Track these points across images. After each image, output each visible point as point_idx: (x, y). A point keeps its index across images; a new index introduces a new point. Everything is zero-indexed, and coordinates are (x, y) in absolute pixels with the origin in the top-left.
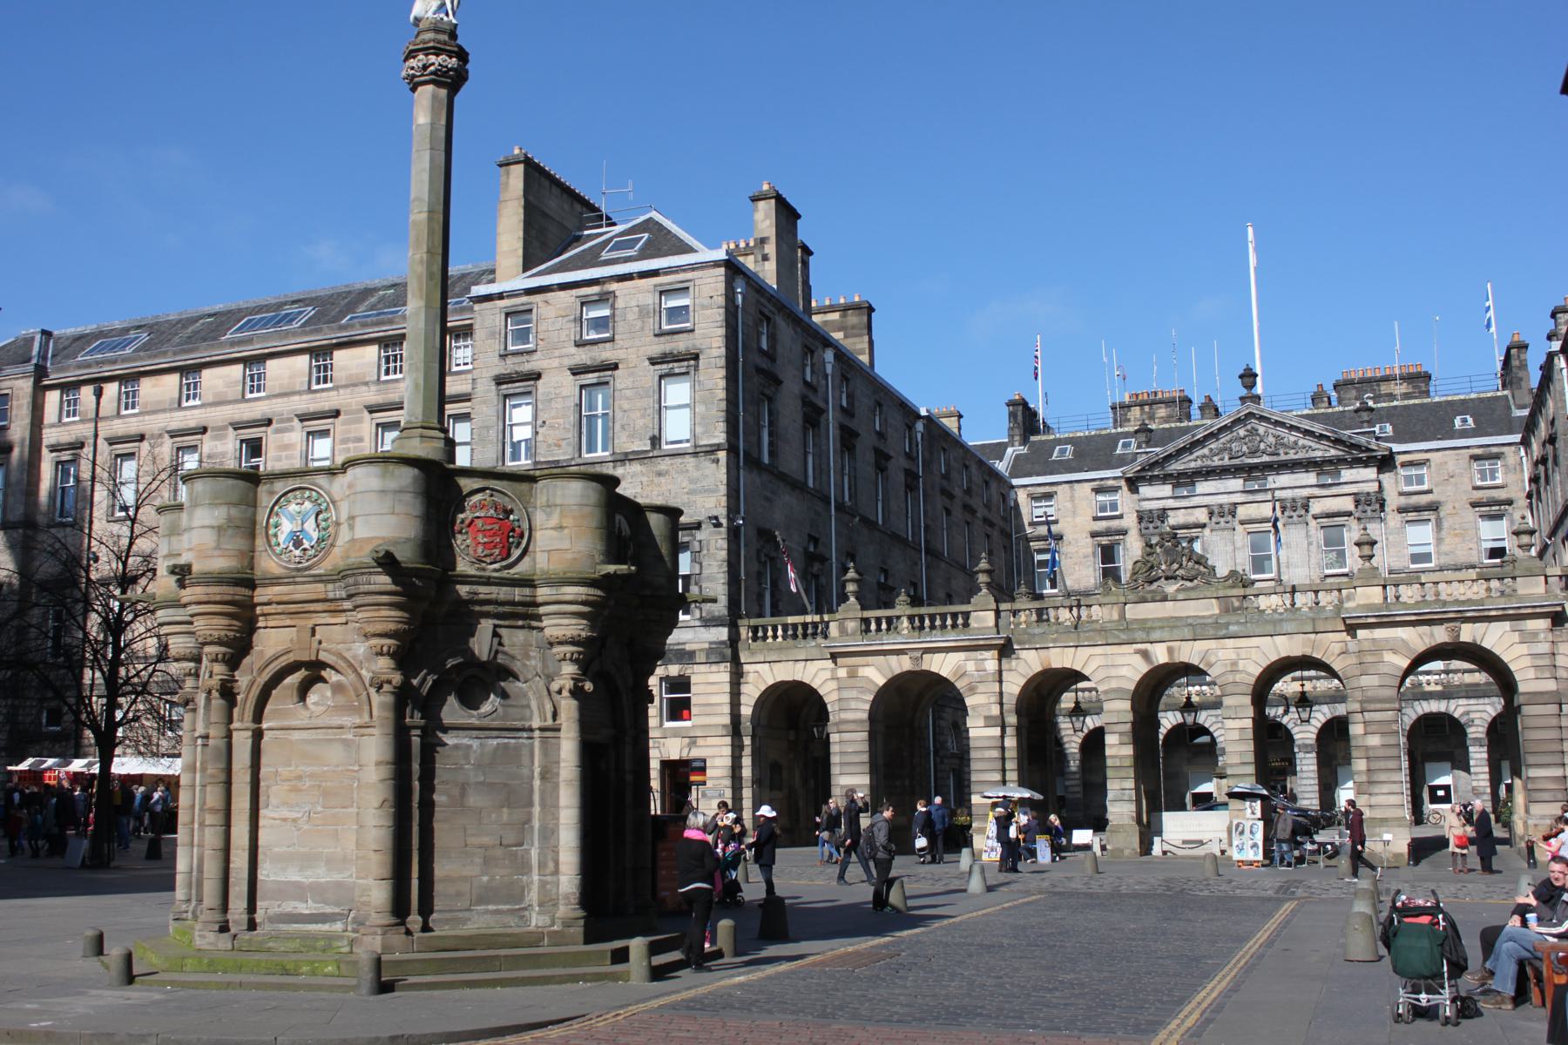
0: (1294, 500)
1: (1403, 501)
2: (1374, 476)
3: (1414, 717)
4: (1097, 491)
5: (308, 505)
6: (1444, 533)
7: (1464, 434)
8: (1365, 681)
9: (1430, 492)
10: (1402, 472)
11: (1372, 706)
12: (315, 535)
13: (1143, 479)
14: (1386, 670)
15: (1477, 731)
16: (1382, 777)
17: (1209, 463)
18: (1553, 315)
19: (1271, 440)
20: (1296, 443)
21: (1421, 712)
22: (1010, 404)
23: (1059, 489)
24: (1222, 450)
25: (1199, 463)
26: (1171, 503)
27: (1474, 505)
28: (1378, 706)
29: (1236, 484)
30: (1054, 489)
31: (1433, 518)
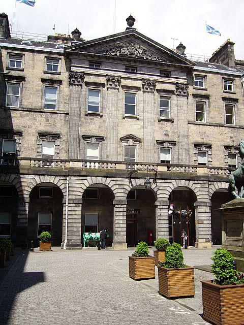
0: (149, 80)
1: (195, 92)
6: (211, 108)
9: (206, 90)
19: (140, 51)
21: (217, 188)
23: (26, 53)
27: (224, 99)
30: (24, 53)
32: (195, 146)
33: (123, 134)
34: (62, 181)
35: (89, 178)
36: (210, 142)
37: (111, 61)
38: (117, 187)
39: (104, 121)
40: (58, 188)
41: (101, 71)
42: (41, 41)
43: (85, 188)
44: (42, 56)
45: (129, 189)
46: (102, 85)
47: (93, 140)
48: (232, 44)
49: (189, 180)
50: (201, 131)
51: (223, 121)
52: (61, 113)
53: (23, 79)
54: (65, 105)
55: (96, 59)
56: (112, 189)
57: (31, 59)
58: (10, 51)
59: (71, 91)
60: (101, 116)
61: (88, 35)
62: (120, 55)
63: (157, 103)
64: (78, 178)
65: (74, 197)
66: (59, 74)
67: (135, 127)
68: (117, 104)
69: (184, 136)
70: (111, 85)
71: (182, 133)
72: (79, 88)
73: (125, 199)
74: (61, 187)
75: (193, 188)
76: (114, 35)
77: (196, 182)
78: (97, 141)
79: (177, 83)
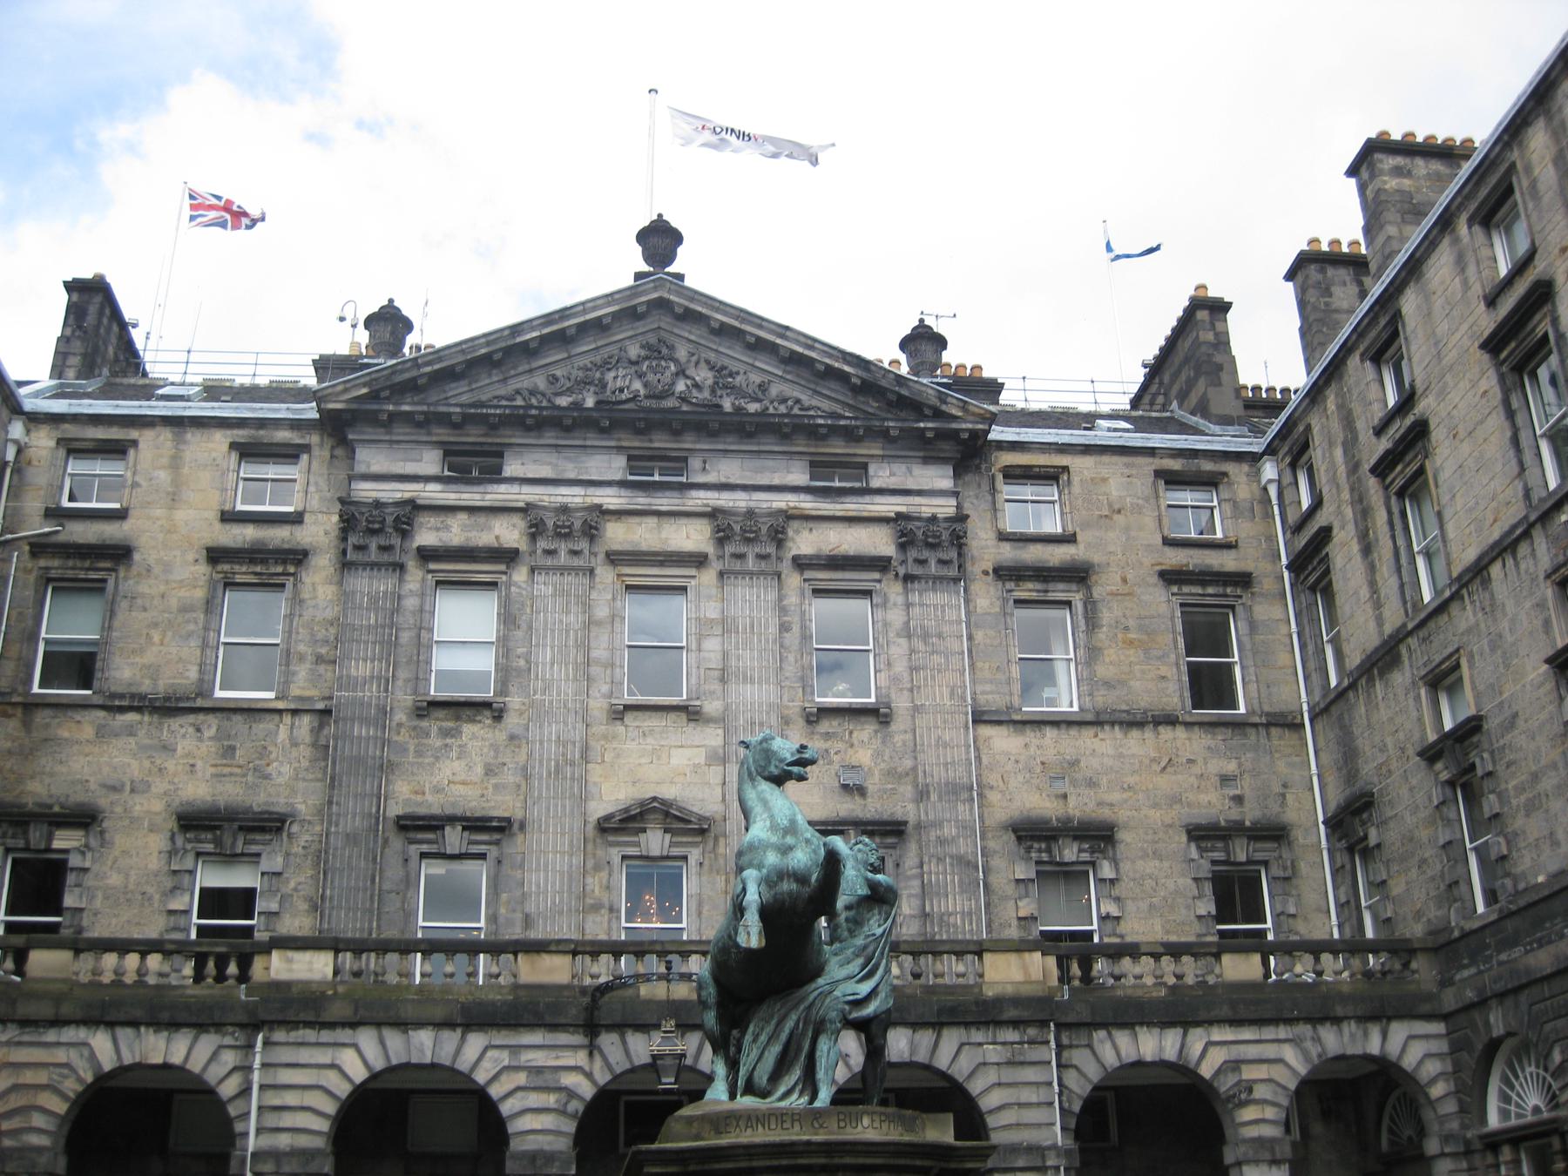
0: (750, 513)
2: (947, 483)
3: (1094, 1073)
4: (247, 452)
6: (1102, 635)
10: (1007, 490)
13: (372, 419)
15: (1258, 1120)
19: (704, 375)
20: (763, 387)
21: (1110, 1059)
22: (72, 286)
23: (146, 438)
26: (433, 493)
27: (1170, 577)
30: (134, 434)
31: (1077, 598)
32: (1019, 839)
33: (612, 796)
34: (229, 1058)
35: (367, 1039)
36: (1105, 814)
37: (549, 437)
38: (521, 1078)
39: (512, 738)
40: (211, 1092)
41: (503, 488)
42: (263, 381)
43: (343, 1090)
44: (220, 441)
45: (587, 1091)
46: (508, 556)
47: (454, 839)
48: (1220, 308)
49: (938, 1025)
50: (1050, 755)
51: (1173, 693)
52: (295, 712)
53: (121, 554)
54: (322, 668)
55: (473, 436)
56: (495, 1091)
57: (165, 461)
58: (71, 430)
59: (345, 598)
60: (498, 716)
61: (438, 327)
62: (598, 403)
63: (796, 629)
64: (310, 1035)
65: (284, 1141)
66: (296, 519)
67: (680, 759)
68: (585, 646)
69: (955, 791)
70: (550, 553)
71: (938, 775)
72: (383, 584)
73: (563, 1144)
74: (228, 1089)
75: (960, 1070)
76: (564, 313)
77: (977, 1036)
78: (470, 843)
79: (900, 516)
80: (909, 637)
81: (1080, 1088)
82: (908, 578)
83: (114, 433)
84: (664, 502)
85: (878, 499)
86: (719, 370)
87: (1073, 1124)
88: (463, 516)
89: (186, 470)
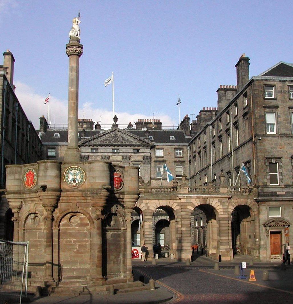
1: (156, 159)
3: (158, 221)
5: (77, 172)
7: (173, 142)
8: (183, 213)
10: (157, 151)
11: (184, 220)
12: (80, 180)
14: (188, 210)
16: (186, 238)
17: (103, 143)
18: (200, 112)
20: (128, 140)
21: (159, 219)
22: (41, 119)
24: (106, 140)
25: (100, 143)
26: (90, 154)
27: (175, 162)
28: (186, 220)
29: (110, 149)
37: (103, 147)
80: (144, 170)
81: (156, 222)
82: (144, 163)
83: (53, 147)
84: (116, 155)
85: (141, 154)
86: (123, 137)
87: (155, 225)
88: (94, 157)
89: (62, 151)
